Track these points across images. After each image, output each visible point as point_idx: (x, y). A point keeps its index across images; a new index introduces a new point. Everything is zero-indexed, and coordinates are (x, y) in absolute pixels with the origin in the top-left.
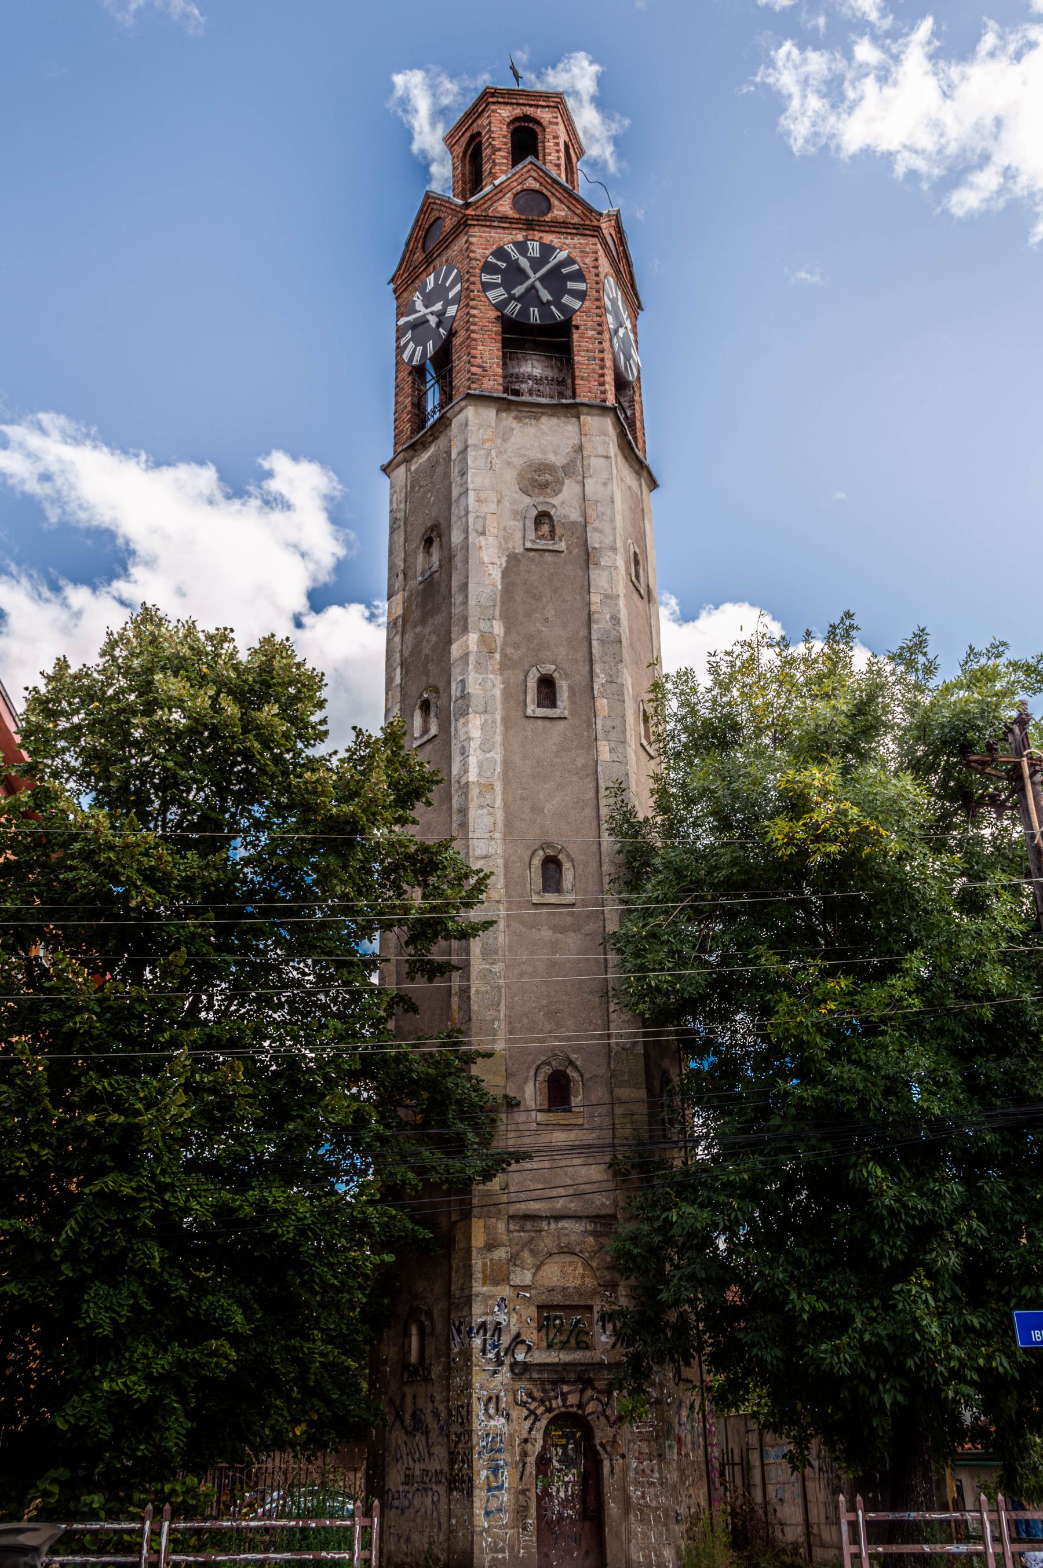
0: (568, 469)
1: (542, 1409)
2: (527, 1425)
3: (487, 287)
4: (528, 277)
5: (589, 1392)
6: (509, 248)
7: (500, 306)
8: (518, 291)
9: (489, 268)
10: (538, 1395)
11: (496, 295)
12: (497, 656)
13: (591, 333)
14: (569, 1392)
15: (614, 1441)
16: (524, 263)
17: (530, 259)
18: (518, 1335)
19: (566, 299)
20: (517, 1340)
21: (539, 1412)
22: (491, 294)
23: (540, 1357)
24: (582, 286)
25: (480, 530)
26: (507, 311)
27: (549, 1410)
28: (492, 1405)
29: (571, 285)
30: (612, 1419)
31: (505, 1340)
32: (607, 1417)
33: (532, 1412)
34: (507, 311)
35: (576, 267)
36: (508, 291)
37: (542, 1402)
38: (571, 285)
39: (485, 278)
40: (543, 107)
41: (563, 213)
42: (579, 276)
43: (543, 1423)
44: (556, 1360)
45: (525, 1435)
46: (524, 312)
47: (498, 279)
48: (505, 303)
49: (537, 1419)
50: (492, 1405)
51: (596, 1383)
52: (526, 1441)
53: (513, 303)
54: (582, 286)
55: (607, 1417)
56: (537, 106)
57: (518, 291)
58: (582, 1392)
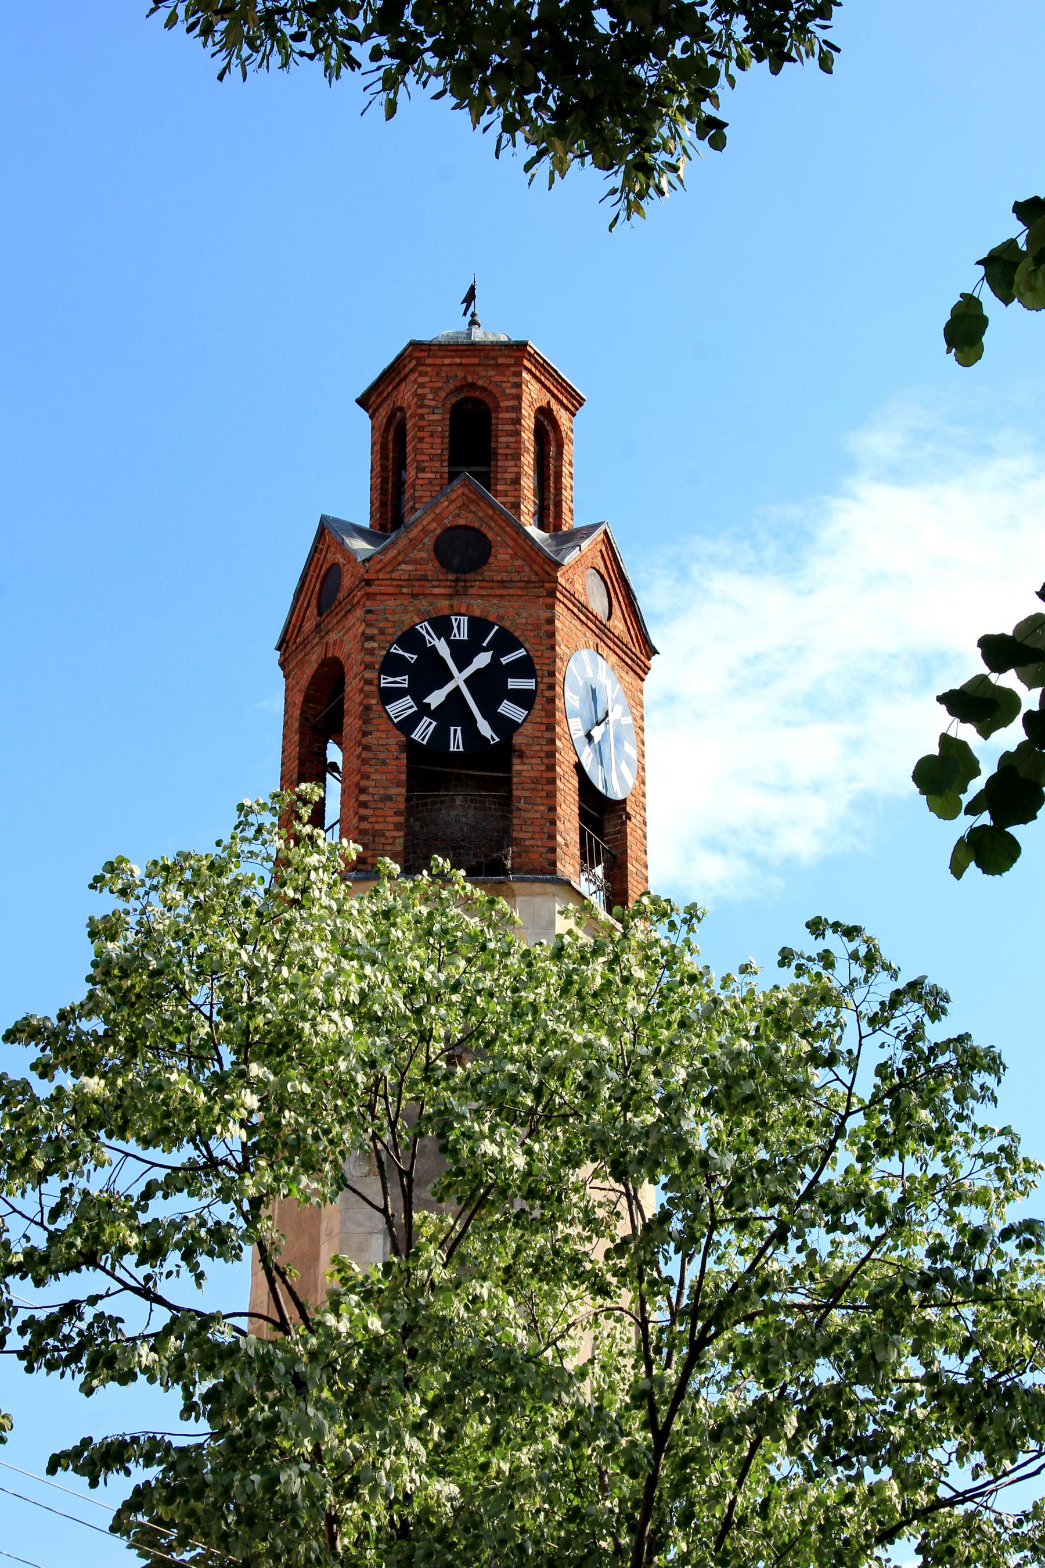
3: (390, 695)
4: (452, 677)
6: (424, 629)
7: (409, 724)
8: (436, 699)
9: (392, 665)
11: (402, 708)
16: (443, 650)
17: (451, 644)
19: (508, 709)
22: (392, 709)
24: (529, 684)
26: (416, 736)
29: (513, 684)
34: (416, 736)
35: (522, 653)
36: (418, 700)
38: (513, 684)
39: (386, 682)
46: (441, 736)
47: (403, 681)
48: (411, 722)
53: (426, 720)
54: (529, 684)
57: (436, 699)
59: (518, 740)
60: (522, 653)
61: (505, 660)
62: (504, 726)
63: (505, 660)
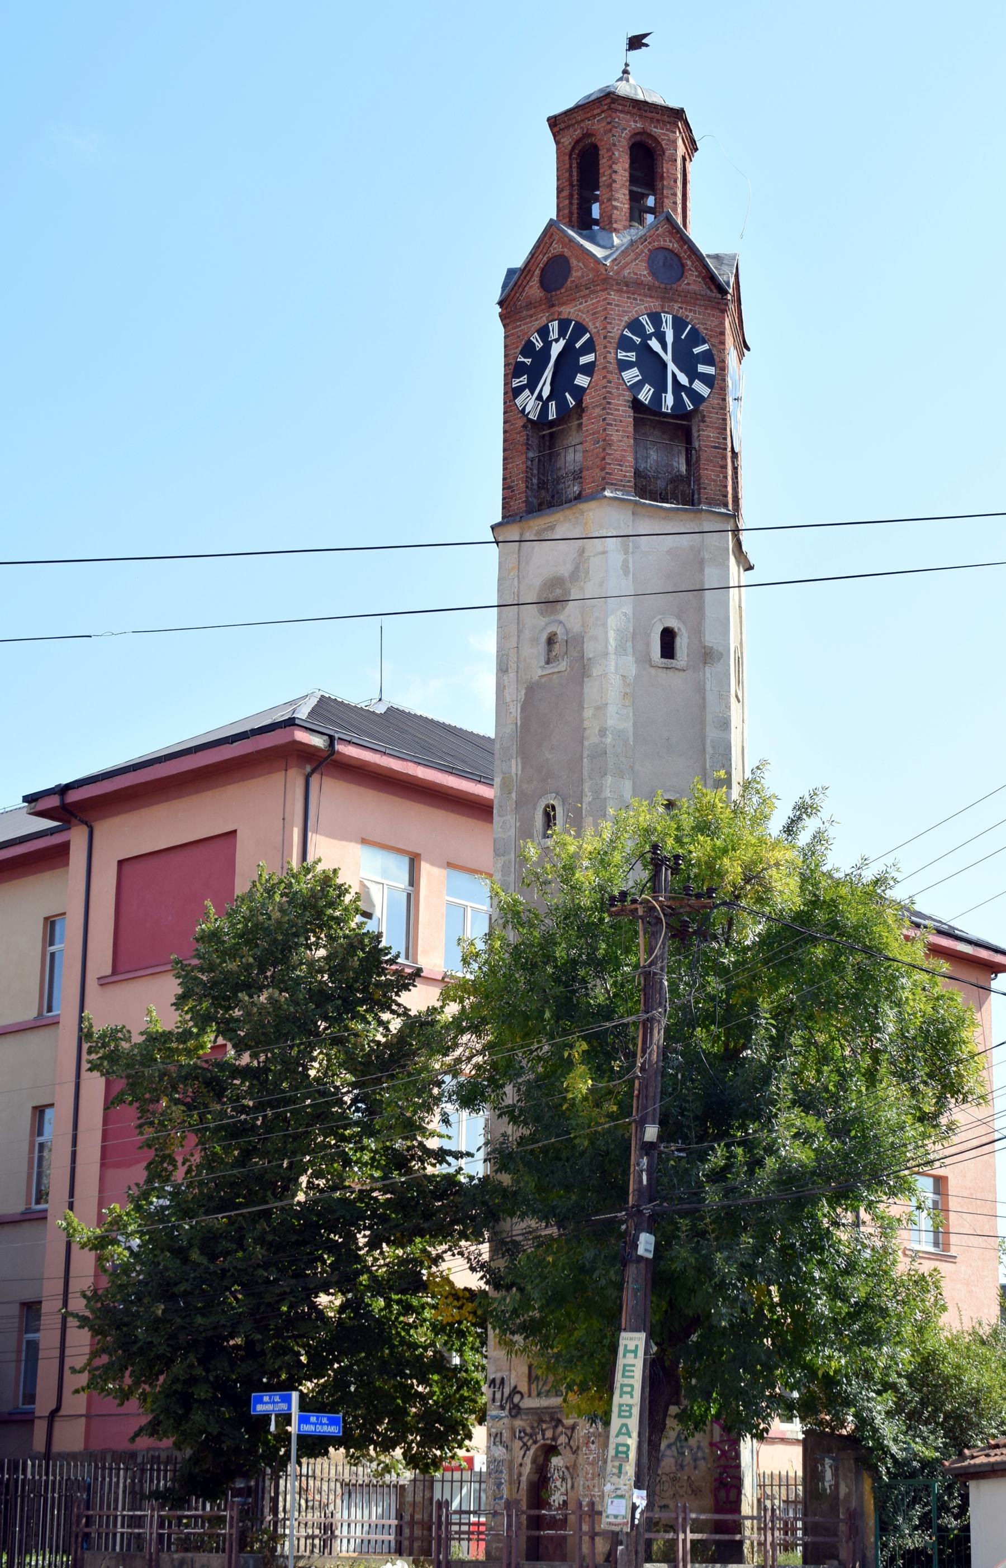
0: (574, 576)
1: (531, 1441)
2: (522, 1452)
5: (560, 1429)
10: (528, 1430)
12: (514, 795)
13: (598, 411)
14: (546, 1429)
15: (575, 1465)
18: (515, 1387)
20: (515, 1391)
21: (529, 1444)
23: (527, 1403)
25: (504, 669)
27: (535, 1442)
28: (498, 1439)
30: (574, 1448)
31: (507, 1391)
32: (571, 1448)
33: (525, 1444)
35: (588, 335)
37: (531, 1436)
40: (599, 114)
41: (579, 274)
42: (589, 347)
43: (530, 1453)
44: (538, 1405)
45: (520, 1460)
49: (528, 1449)
50: (498, 1439)
51: (565, 1421)
52: (521, 1465)
55: (571, 1448)
56: (594, 116)
58: (556, 1426)
59: (587, 400)
60: (588, 335)
61: (578, 345)
62: (579, 392)
63: (578, 345)
